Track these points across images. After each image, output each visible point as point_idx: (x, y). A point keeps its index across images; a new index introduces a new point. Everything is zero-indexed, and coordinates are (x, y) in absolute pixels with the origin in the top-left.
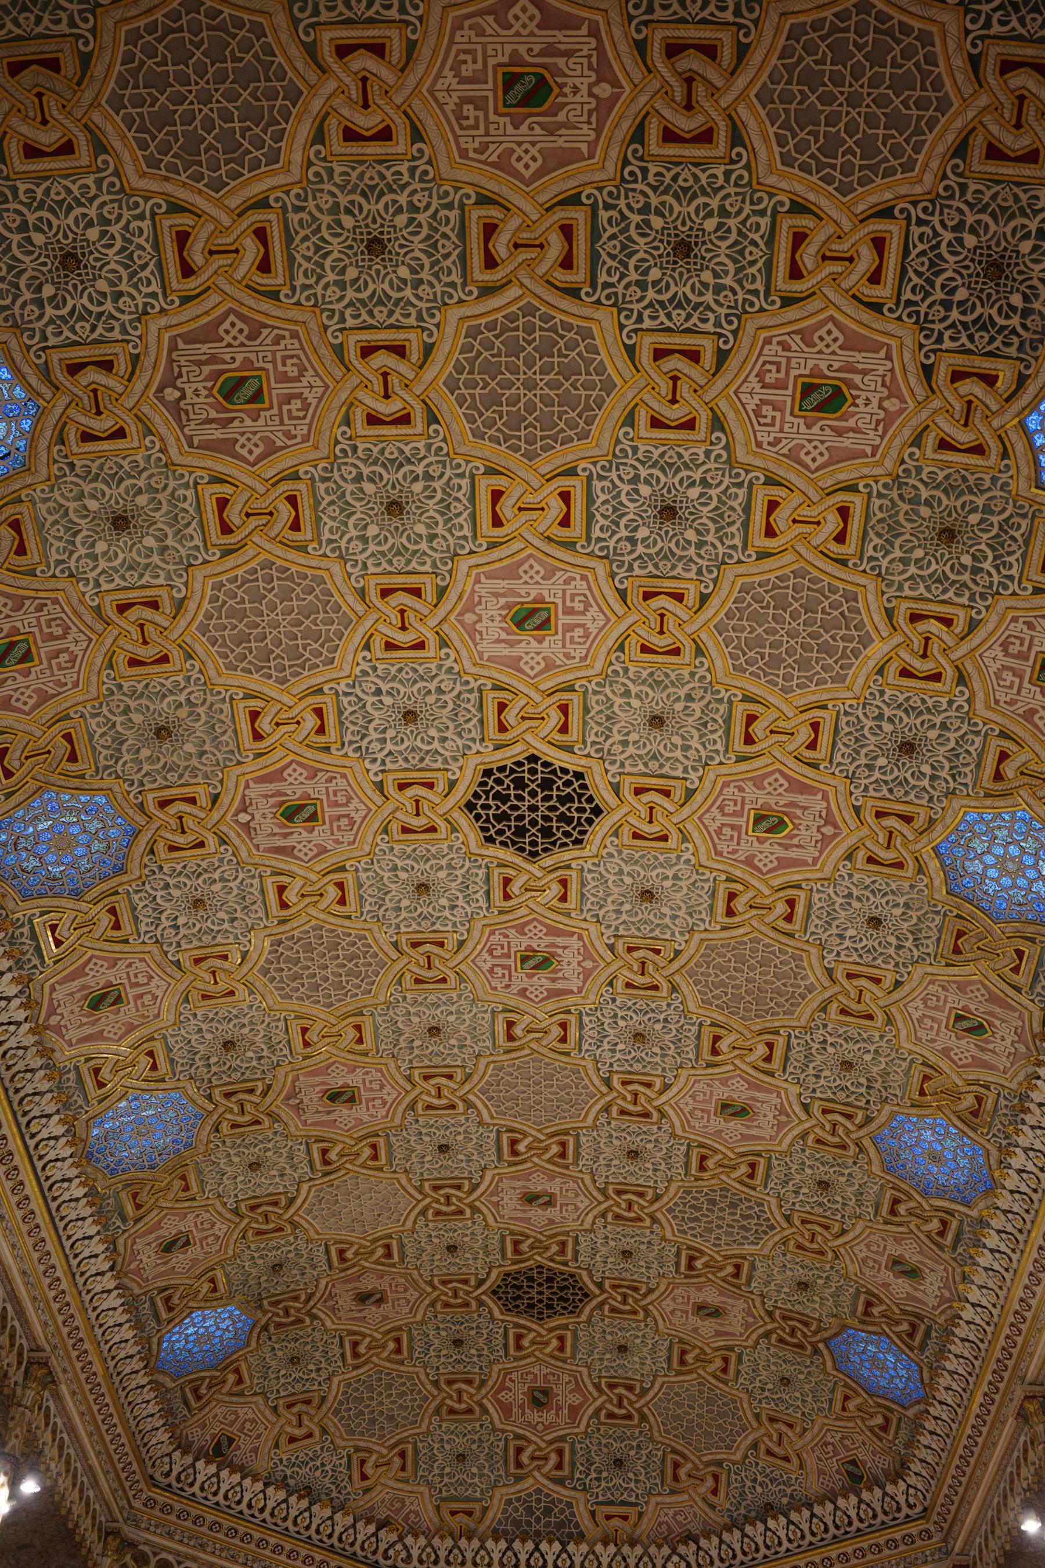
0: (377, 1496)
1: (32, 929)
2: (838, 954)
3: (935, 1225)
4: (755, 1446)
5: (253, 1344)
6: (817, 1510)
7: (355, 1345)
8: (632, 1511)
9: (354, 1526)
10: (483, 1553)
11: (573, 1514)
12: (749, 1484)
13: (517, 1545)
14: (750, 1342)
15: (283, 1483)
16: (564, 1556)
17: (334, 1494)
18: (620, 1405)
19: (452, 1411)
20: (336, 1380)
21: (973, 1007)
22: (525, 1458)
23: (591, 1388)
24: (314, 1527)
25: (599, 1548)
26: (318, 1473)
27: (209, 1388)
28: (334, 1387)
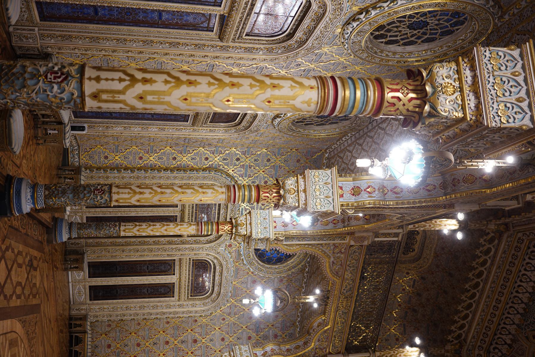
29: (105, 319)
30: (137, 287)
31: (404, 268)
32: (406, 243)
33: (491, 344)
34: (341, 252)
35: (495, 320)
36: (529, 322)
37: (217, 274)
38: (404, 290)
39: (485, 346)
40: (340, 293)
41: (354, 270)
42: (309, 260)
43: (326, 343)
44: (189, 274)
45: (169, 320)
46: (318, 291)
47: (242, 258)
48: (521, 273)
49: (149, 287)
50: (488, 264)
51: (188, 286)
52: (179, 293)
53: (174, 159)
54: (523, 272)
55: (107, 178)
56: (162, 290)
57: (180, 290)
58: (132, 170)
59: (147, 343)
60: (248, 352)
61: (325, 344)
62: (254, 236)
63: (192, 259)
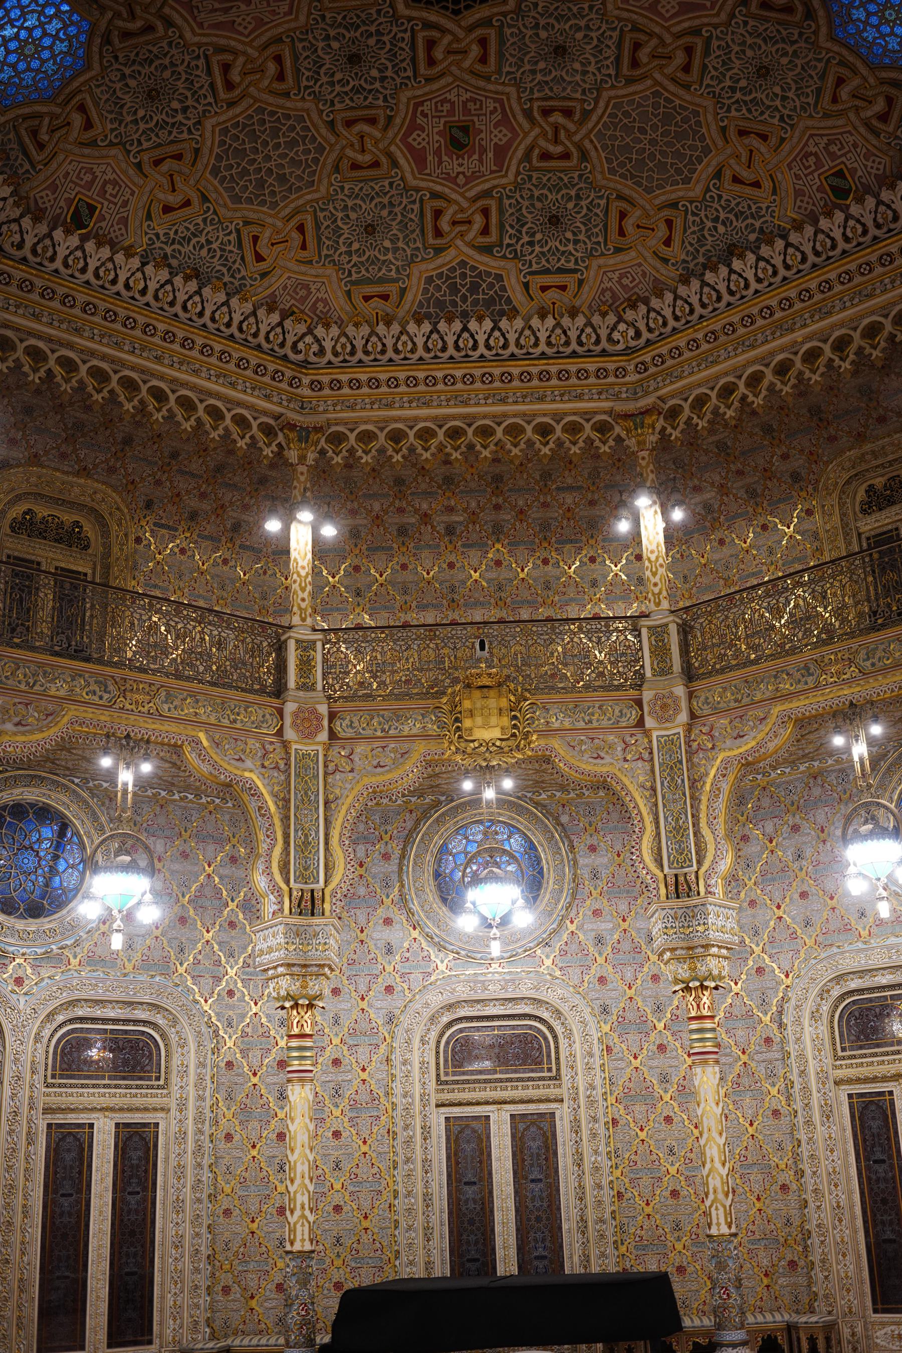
0: (276, 283)
4: (718, 175)
5: (96, 66)
6: (794, 238)
7: (226, 68)
8: (569, 280)
9: (254, 314)
10: (404, 338)
11: (503, 289)
12: (709, 224)
13: (442, 326)
14: (723, 17)
15: (164, 261)
16: (497, 334)
17: (227, 279)
18: (556, 141)
19: (355, 166)
20: (209, 124)
23: (521, 118)
24: (208, 313)
25: (535, 322)
26: (204, 252)
27: (52, 131)
28: (208, 134)
29: (204, 1300)
30: (122, 1221)
31: (122, 550)
32: (56, 541)
33: (285, 358)
35: (218, 347)
36: (225, 270)
37: (98, 1013)
38: (183, 551)
39: (289, 373)
40: (110, 707)
41: (45, 673)
42: (77, 781)
43: (251, 742)
44: (94, 1086)
45: (221, 1135)
46: (106, 762)
47: (56, 951)
48: (93, 281)
49: (123, 1190)
50: (71, 354)
51: (127, 1087)
52: (146, 1109)
54: (89, 276)
56: (135, 1155)
57: (138, 1110)
59: (279, 1189)
60: (266, 932)
63: (50, 1080)
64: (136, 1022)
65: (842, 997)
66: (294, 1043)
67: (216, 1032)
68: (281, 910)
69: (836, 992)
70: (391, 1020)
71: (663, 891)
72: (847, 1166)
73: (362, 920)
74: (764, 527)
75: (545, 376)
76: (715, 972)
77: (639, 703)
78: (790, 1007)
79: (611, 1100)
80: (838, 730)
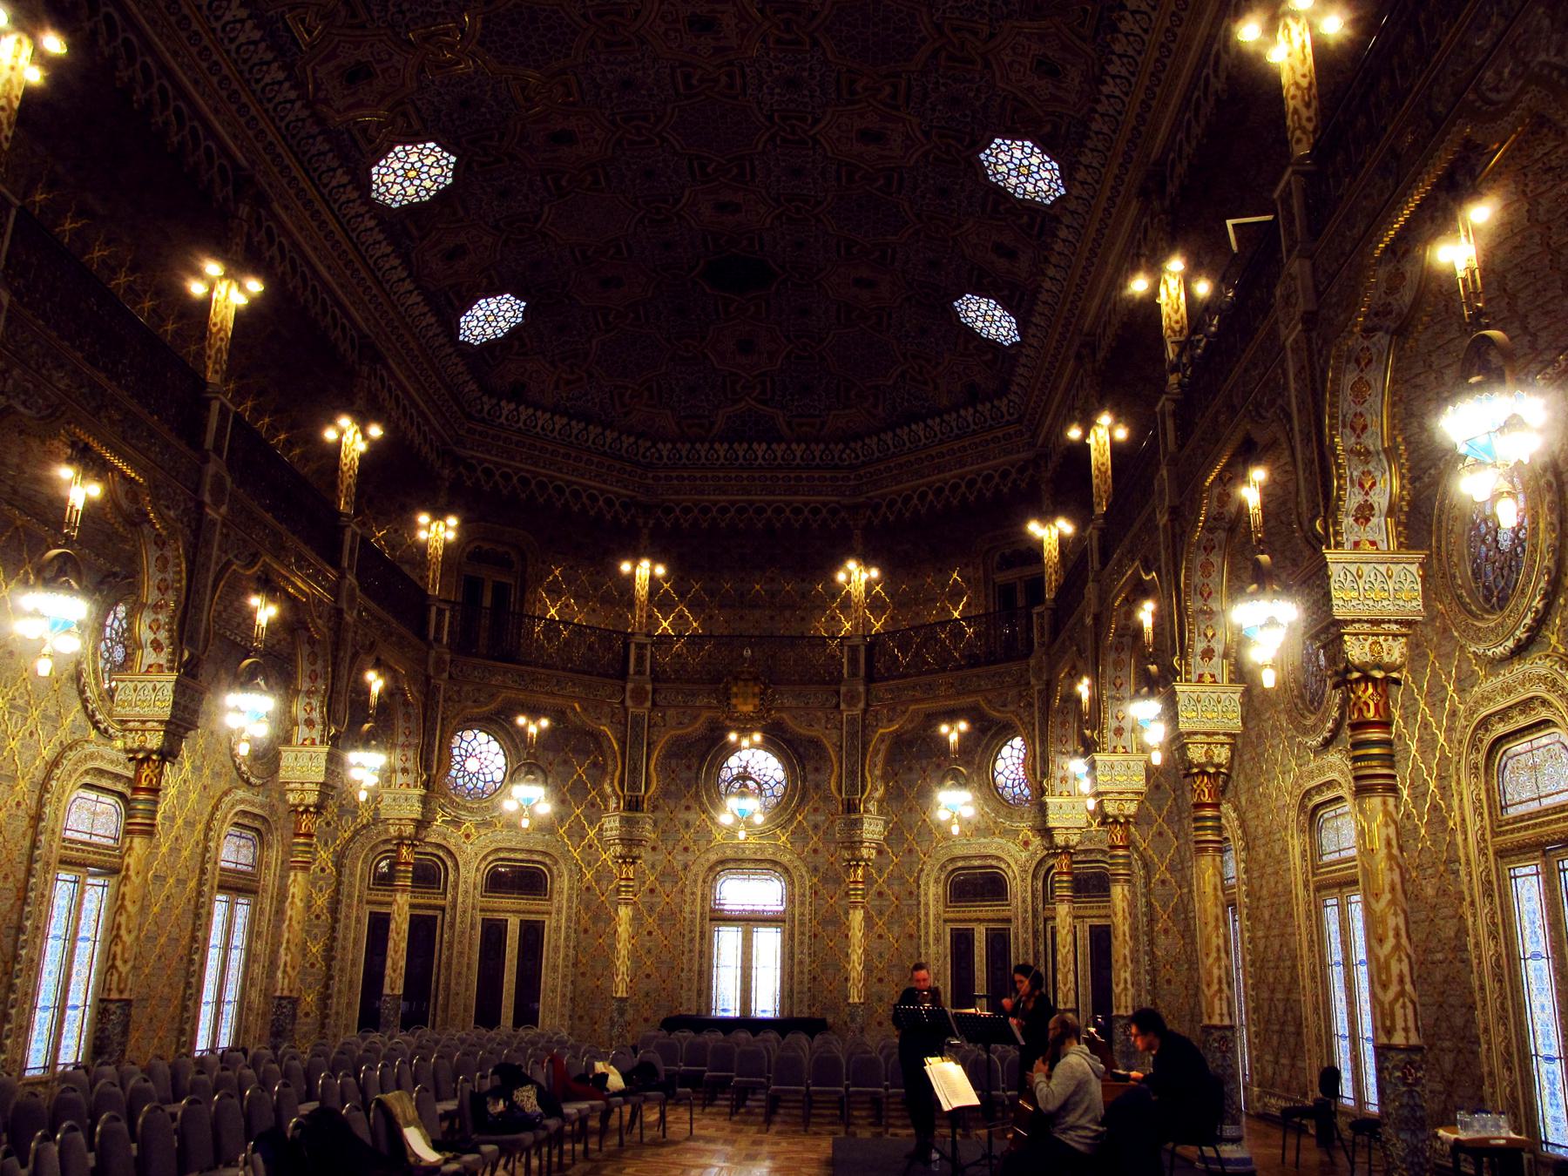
1: (285, 23)
2: (944, 12)
3: (1025, 219)
20: (594, 342)
21: (1050, 54)
22: (738, 388)
25: (794, 446)
34: (459, 692)
35: (596, 460)
37: (512, 856)
39: (639, 471)
45: (581, 929)
53: (318, 917)
55: (337, 1013)
58: (331, 978)
61: (607, 709)
62: (415, 816)
64: (534, 862)
65: (953, 871)
66: (623, 883)
67: (581, 869)
68: (618, 807)
69: (950, 868)
70: (686, 867)
71: (840, 808)
72: (945, 969)
73: (672, 807)
74: (940, 570)
75: (798, 479)
76: (866, 856)
77: (838, 693)
78: (923, 875)
79: (814, 923)
80: (944, 720)
